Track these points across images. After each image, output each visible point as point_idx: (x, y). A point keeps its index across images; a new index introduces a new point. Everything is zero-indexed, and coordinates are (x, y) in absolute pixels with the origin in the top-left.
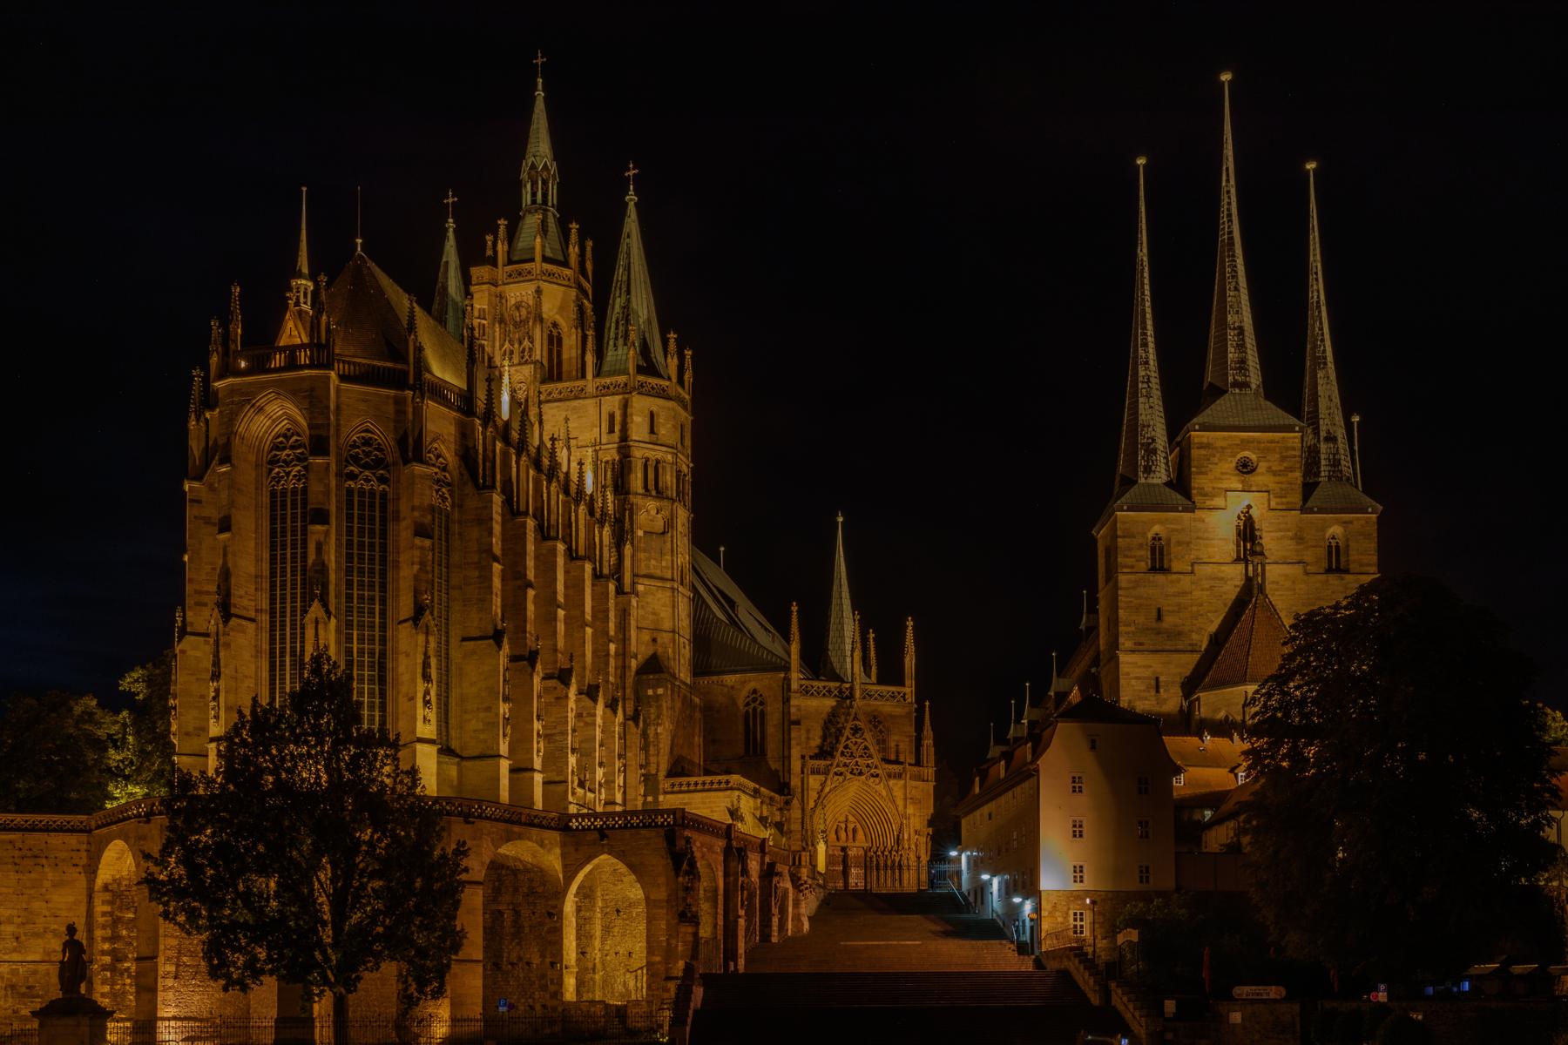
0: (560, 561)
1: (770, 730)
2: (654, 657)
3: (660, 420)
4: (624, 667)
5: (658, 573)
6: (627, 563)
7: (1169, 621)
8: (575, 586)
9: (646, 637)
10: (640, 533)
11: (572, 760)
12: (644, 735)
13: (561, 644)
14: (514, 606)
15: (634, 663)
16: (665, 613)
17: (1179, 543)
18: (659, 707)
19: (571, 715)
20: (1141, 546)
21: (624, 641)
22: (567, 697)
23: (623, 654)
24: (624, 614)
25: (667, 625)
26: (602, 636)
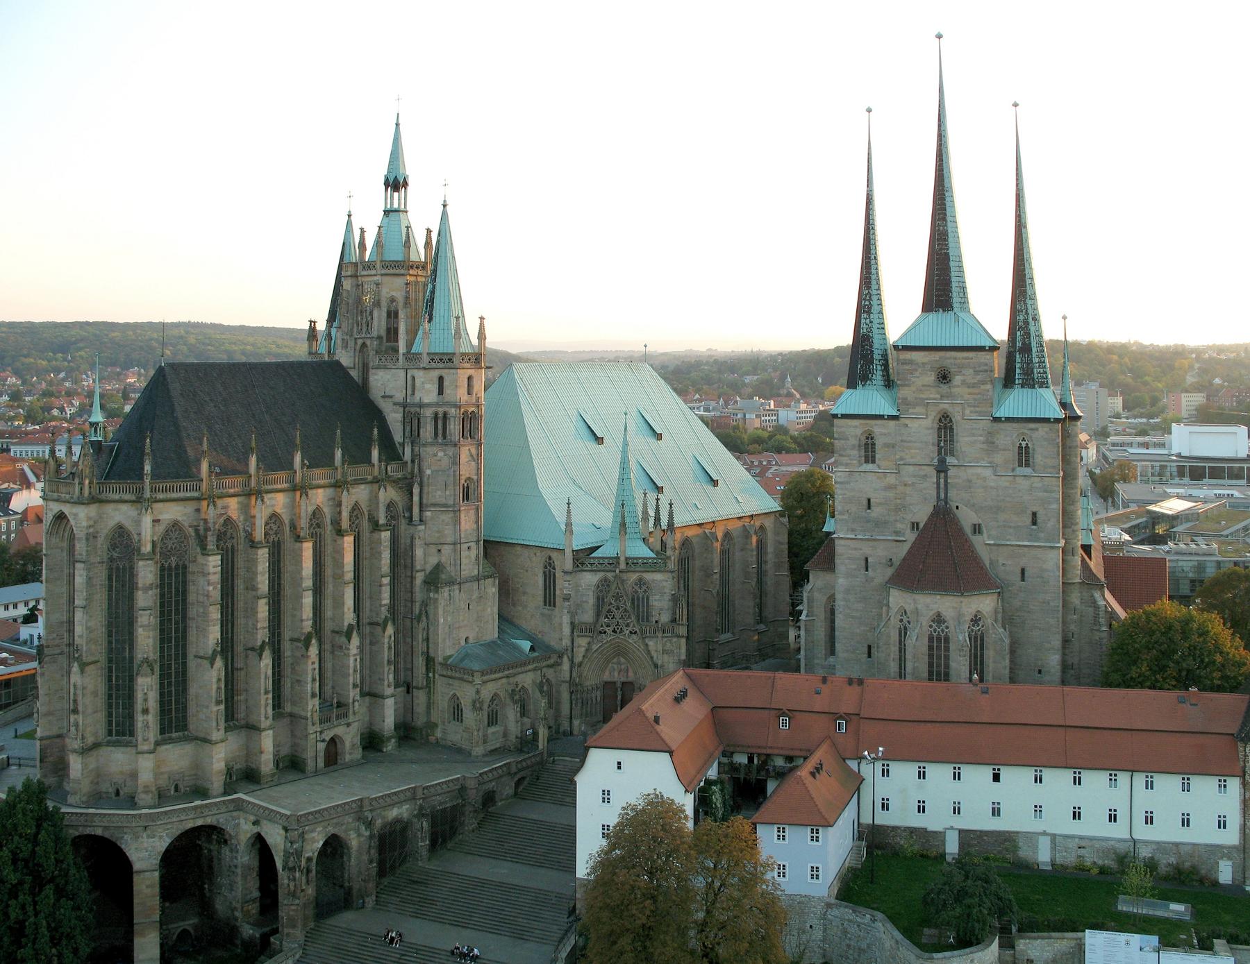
2: (438, 568)
3: (446, 383)
5: (443, 501)
6: (416, 498)
7: (876, 512)
10: (428, 472)
15: (420, 577)
17: (887, 445)
18: (436, 608)
20: (853, 447)
22: (307, 657)
25: (450, 539)
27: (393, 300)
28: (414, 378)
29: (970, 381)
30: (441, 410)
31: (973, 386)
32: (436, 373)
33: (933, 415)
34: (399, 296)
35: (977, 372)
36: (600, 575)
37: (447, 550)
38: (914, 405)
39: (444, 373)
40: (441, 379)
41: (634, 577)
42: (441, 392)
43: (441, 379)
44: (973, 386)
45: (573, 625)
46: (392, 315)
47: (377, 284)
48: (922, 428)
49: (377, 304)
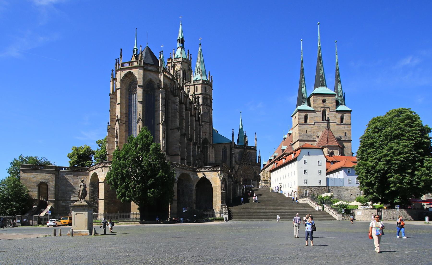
0: (189, 115)
1: (228, 155)
2: (206, 138)
4: (200, 140)
5: (206, 121)
8: (192, 121)
9: (204, 134)
11: (192, 158)
12: (204, 155)
13: (189, 133)
14: (181, 123)
16: (208, 129)
19: (192, 148)
21: (200, 135)
23: (200, 137)
24: (200, 129)
25: (208, 132)
26: (196, 132)
27: (184, 70)
28: (197, 87)
29: (330, 102)
30: (206, 96)
31: (331, 103)
32: (204, 86)
33: (322, 109)
34: (186, 68)
35: (332, 100)
36: (240, 150)
37: (208, 134)
38: (317, 108)
39: (207, 86)
40: (205, 88)
41: (248, 151)
42: (205, 91)
43: (205, 88)
44: (331, 103)
45: (235, 162)
46: (184, 74)
47: (181, 64)
48: (320, 114)
49: (181, 69)
